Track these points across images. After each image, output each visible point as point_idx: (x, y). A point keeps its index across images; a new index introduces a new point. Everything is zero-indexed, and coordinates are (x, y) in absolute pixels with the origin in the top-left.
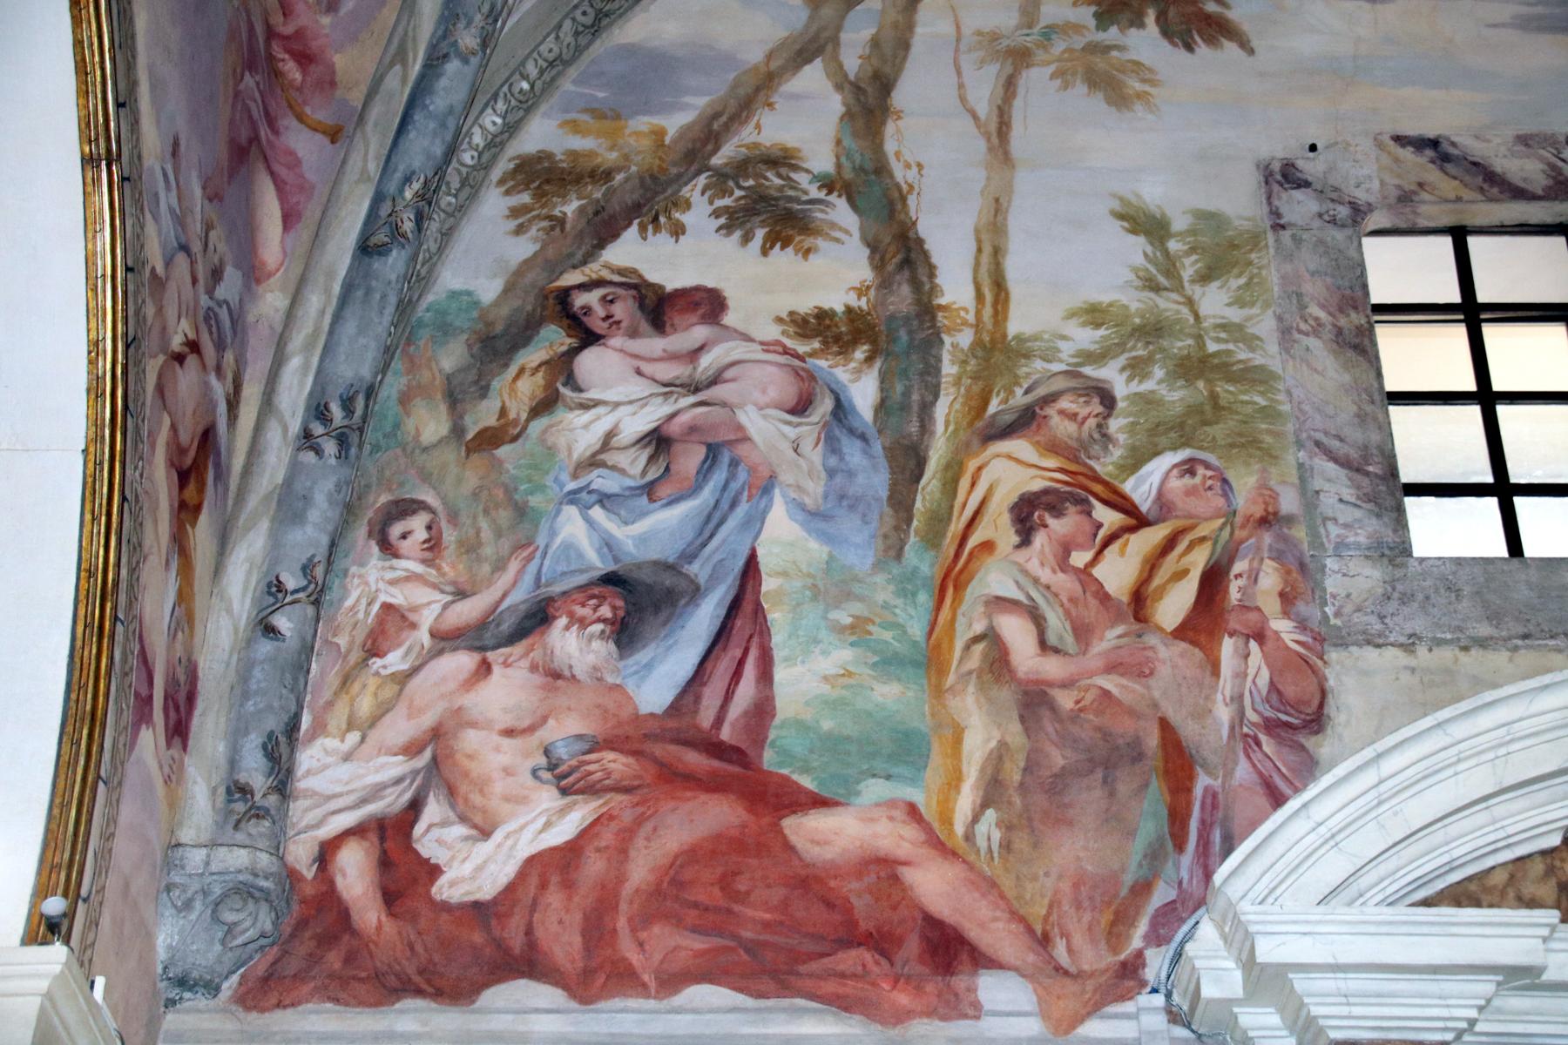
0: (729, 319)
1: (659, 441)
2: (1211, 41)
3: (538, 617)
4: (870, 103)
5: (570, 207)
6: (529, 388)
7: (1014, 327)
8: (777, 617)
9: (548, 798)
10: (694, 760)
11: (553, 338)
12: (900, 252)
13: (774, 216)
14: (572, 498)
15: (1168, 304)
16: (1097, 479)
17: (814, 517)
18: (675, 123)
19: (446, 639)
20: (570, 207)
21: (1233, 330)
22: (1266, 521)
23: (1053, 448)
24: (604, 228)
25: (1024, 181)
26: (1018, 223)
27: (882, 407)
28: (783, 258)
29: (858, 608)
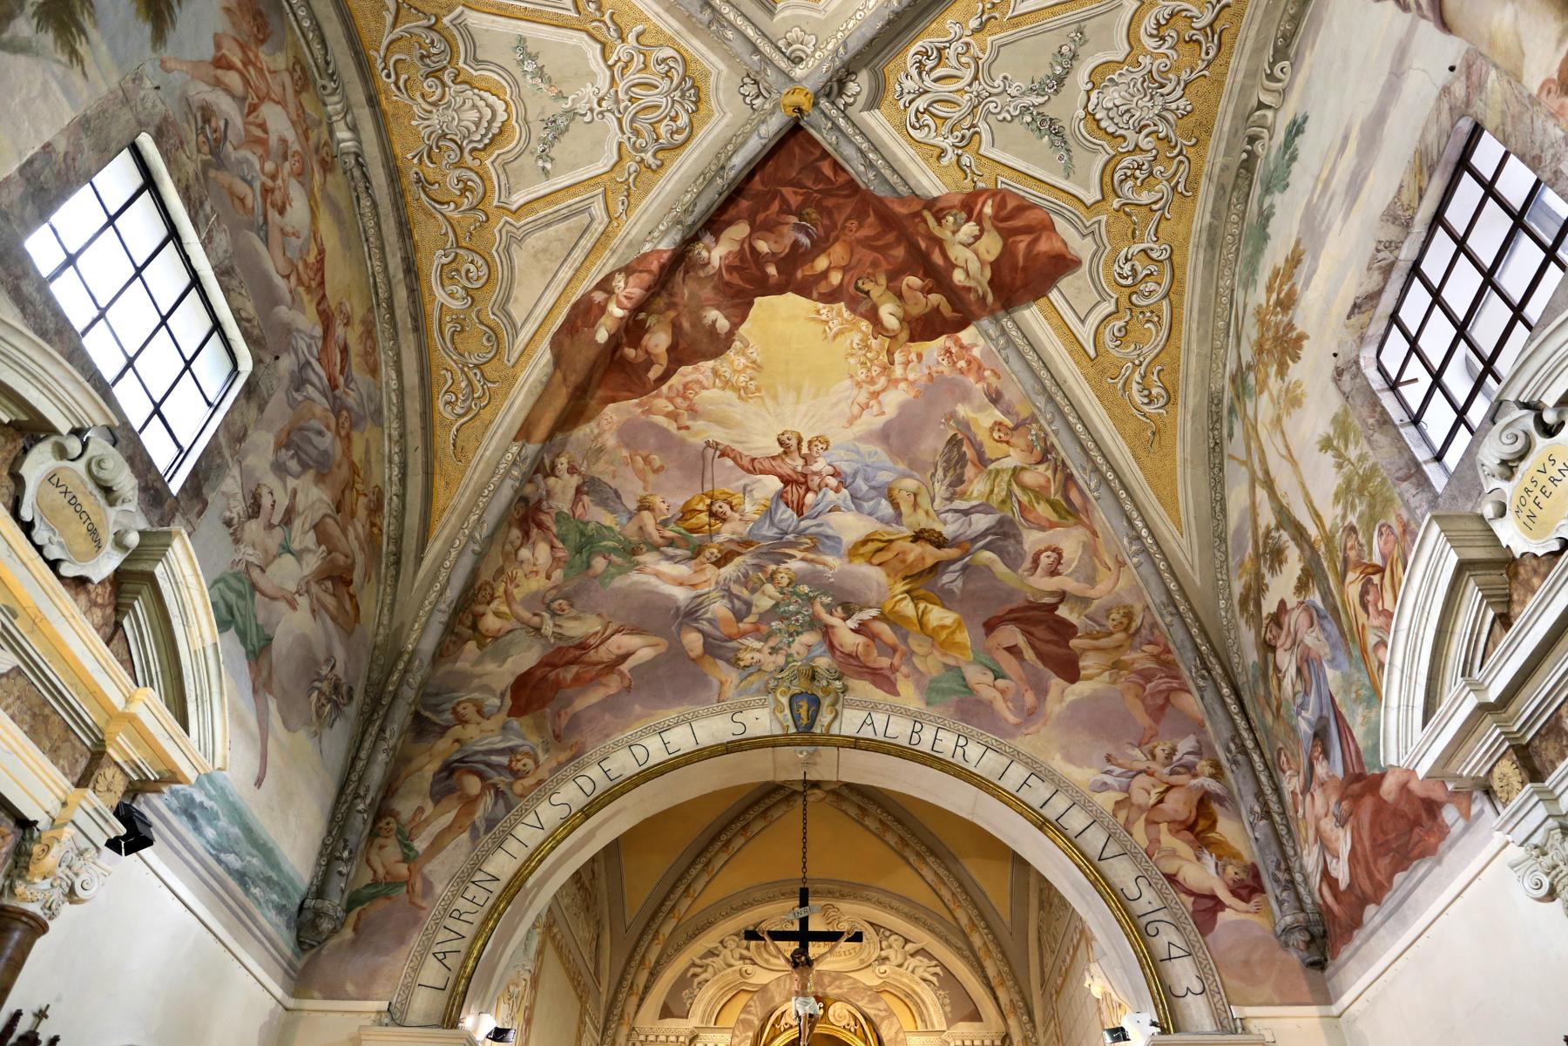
0: (1289, 606)
1: (1299, 671)
2: (1301, 348)
3: (1311, 766)
4: (1269, 484)
5: (1252, 608)
6: (1274, 682)
7: (1328, 526)
8: (1343, 711)
9: (1341, 832)
10: (1356, 787)
11: (1270, 656)
12: (1299, 533)
13: (1277, 556)
14: (1298, 714)
15: (1347, 468)
16: (1369, 566)
17: (1332, 661)
18: (1250, 550)
19: (1303, 793)
20: (1252, 608)
21: (1362, 458)
22: (1404, 531)
23: (1356, 567)
24: (1258, 606)
25: (1301, 466)
26: (1308, 484)
27: (1324, 600)
28: (1285, 568)
29: (1354, 688)
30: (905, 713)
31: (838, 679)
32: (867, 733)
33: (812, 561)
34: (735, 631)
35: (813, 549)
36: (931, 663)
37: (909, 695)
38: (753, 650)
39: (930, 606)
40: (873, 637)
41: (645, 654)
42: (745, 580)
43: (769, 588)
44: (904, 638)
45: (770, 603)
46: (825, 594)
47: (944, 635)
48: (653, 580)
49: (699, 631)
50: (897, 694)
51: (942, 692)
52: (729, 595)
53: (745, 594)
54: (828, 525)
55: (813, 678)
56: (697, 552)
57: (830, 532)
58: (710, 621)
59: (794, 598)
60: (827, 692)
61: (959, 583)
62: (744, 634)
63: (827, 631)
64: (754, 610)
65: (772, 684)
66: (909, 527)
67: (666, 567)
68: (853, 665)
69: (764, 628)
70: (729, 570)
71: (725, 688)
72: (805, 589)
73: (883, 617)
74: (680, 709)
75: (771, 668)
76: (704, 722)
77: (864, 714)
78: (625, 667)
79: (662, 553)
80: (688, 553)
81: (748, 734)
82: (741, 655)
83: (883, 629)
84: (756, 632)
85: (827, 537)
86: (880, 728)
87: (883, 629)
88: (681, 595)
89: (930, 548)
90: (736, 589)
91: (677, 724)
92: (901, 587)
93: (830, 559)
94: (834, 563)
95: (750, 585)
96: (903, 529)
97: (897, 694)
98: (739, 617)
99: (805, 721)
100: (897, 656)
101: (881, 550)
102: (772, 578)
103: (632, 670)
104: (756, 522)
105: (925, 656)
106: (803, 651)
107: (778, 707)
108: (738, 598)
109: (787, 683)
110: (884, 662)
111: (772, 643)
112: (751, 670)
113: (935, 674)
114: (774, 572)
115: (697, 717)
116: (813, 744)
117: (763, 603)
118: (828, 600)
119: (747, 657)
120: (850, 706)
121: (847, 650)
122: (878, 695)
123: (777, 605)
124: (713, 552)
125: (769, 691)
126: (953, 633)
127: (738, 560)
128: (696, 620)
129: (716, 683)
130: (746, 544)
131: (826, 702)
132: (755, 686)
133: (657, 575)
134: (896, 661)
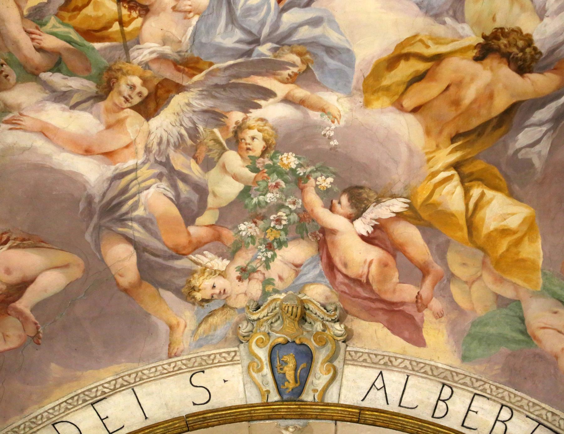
30: (430, 372)
31: (339, 320)
32: (376, 401)
33: (300, 103)
34: (182, 240)
35: (303, 77)
36: (476, 294)
37: (439, 344)
38: (214, 272)
39: (489, 193)
40: (394, 249)
41: (51, 282)
42: (192, 143)
43: (232, 158)
44: (441, 251)
45: (238, 187)
46: (323, 170)
47: (504, 245)
48: (40, 143)
49: (129, 240)
50: (420, 342)
51: (486, 340)
52: (170, 174)
53: (194, 170)
54: (332, 22)
55: (303, 319)
56: (106, 86)
57: (334, 38)
58: (143, 222)
59: (274, 179)
60: (322, 341)
61: (544, 148)
62: (197, 246)
63: (323, 238)
64: (211, 201)
65: (245, 328)
66: (476, 24)
67: (56, 115)
68: (362, 297)
69: (228, 235)
70: (165, 123)
71: (178, 335)
72: (290, 160)
73: (411, 215)
74: (116, 368)
75: (241, 302)
76: (152, 387)
77: (373, 373)
78: (25, 303)
79: (45, 85)
80: (90, 86)
81: (215, 404)
82: (197, 281)
83: (410, 234)
84: (215, 241)
85: (330, 50)
86: (394, 394)
87: (410, 234)
88: (92, 172)
89: (506, 72)
90: (179, 161)
91: (115, 391)
92: (446, 156)
93: (334, 100)
94: (339, 106)
95: (202, 153)
96: (465, 29)
97: (420, 342)
98: (190, 218)
99: (291, 385)
100: (429, 281)
101: (419, 78)
102: (236, 140)
103: (35, 308)
104: (203, 15)
105: (470, 283)
106: (288, 273)
107: (253, 365)
108: (185, 179)
109: (265, 328)
110: (408, 292)
111: (241, 261)
112: (213, 306)
113: (480, 312)
114: (240, 128)
115: (141, 380)
116: (301, 416)
117: (225, 190)
118: (326, 182)
119: (205, 285)
120: (355, 362)
121: (353, 272)
122: (394, 344)
123: (246, 192)
124: (132, 84)
125: (243, 340)
126: (518, 243)
127: (178, 101)
128: (122, 220)
129: (163, 328)
130: (189, 65)
131: (321, 356)
132: (220, 332)
133: (45, 132)
134: (426, 290)
